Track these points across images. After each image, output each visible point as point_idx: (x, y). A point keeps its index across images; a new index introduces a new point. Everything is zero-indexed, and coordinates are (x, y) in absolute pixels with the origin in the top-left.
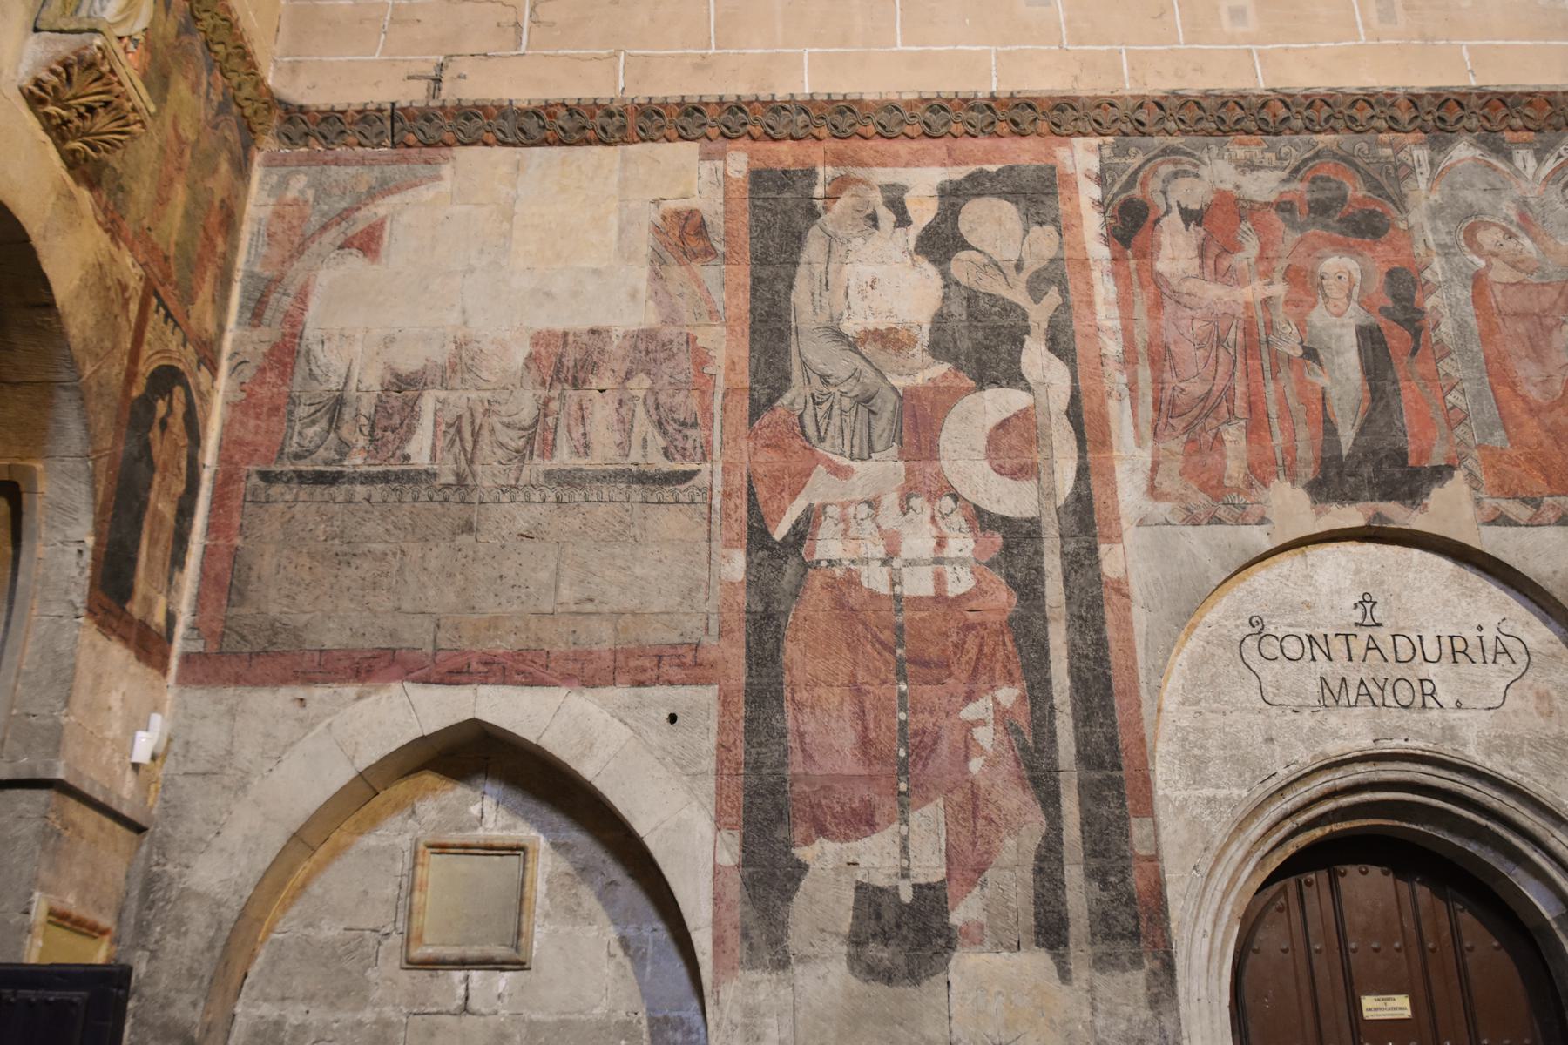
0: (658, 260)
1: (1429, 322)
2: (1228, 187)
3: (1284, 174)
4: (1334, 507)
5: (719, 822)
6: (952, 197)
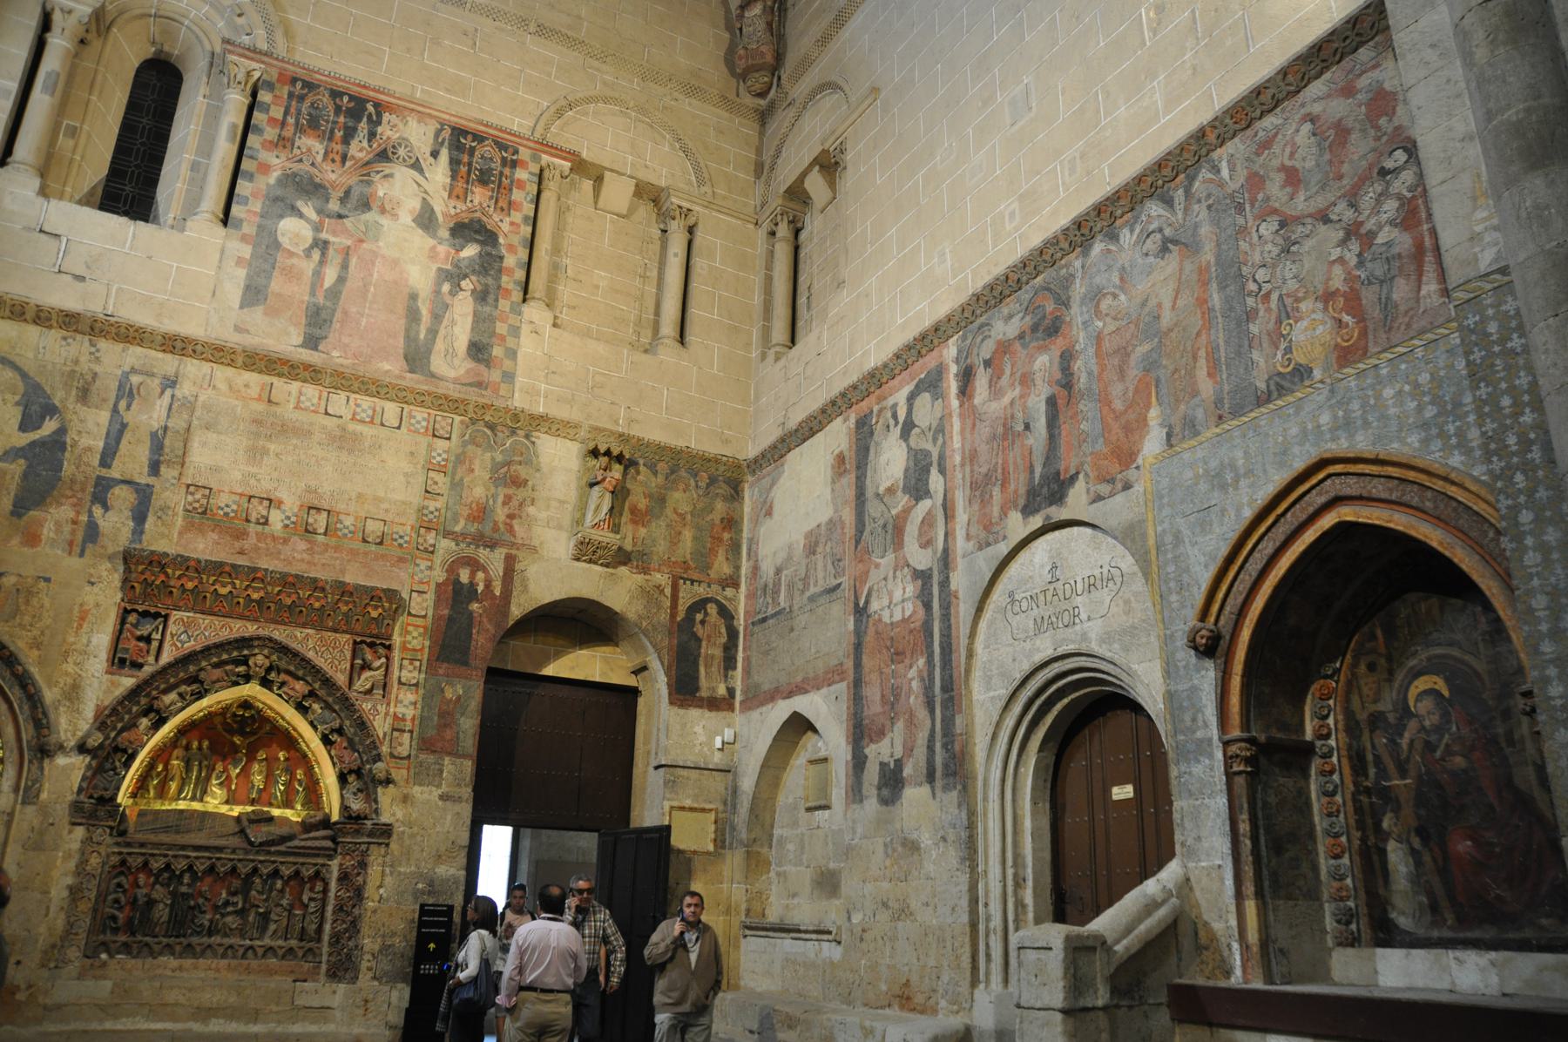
0: (833, 482)
1: (1075, 381)
2: (1001, 336)
3: (1021, 315)
4: (1031, 519)
5: (848, 743)
6: (911, 398)
